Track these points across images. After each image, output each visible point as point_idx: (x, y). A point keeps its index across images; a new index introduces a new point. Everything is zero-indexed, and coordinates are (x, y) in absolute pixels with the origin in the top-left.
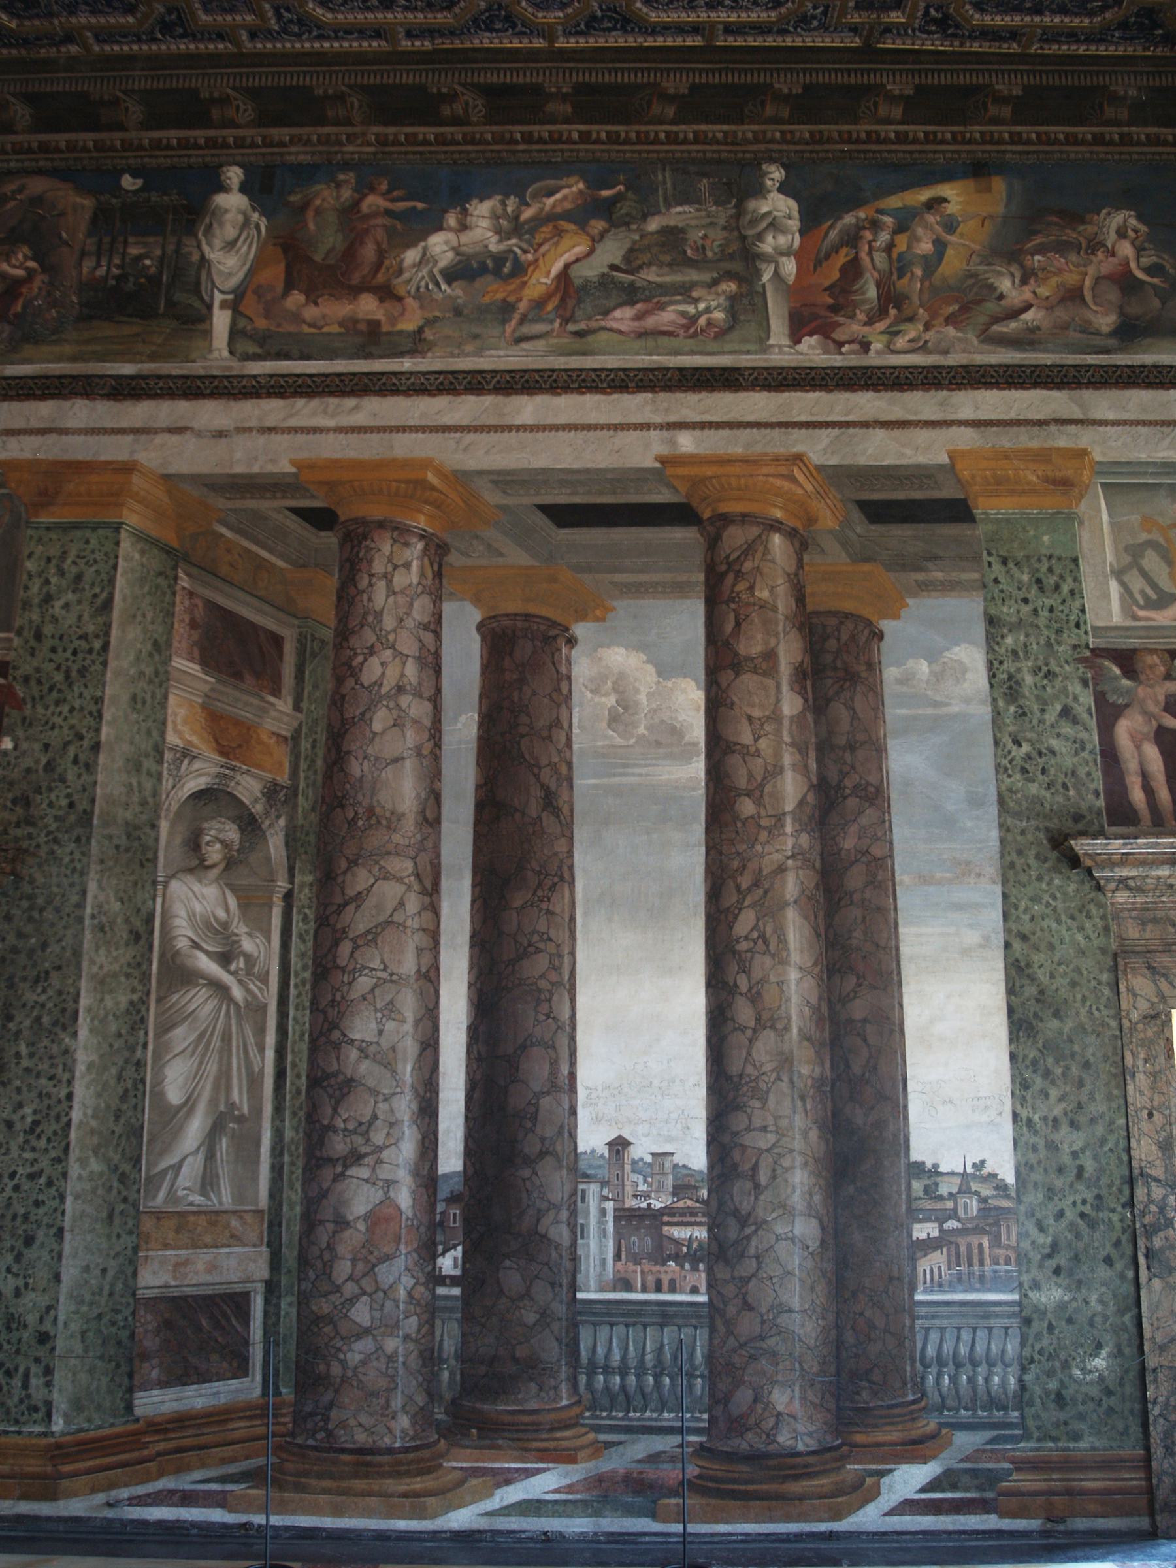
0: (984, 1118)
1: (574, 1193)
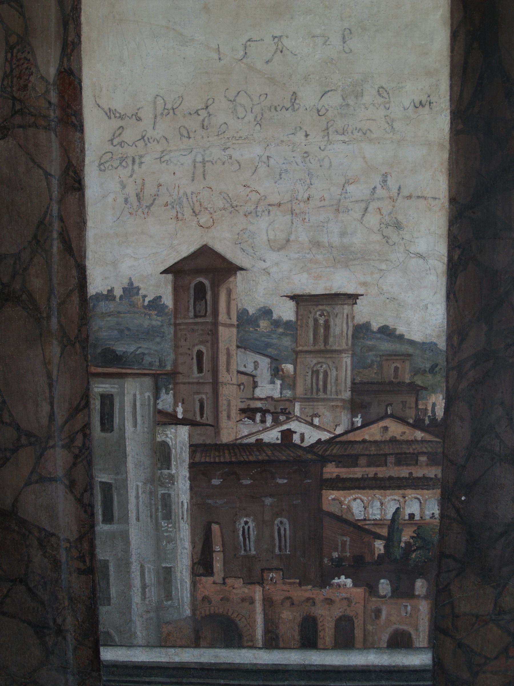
1: (82, 403)
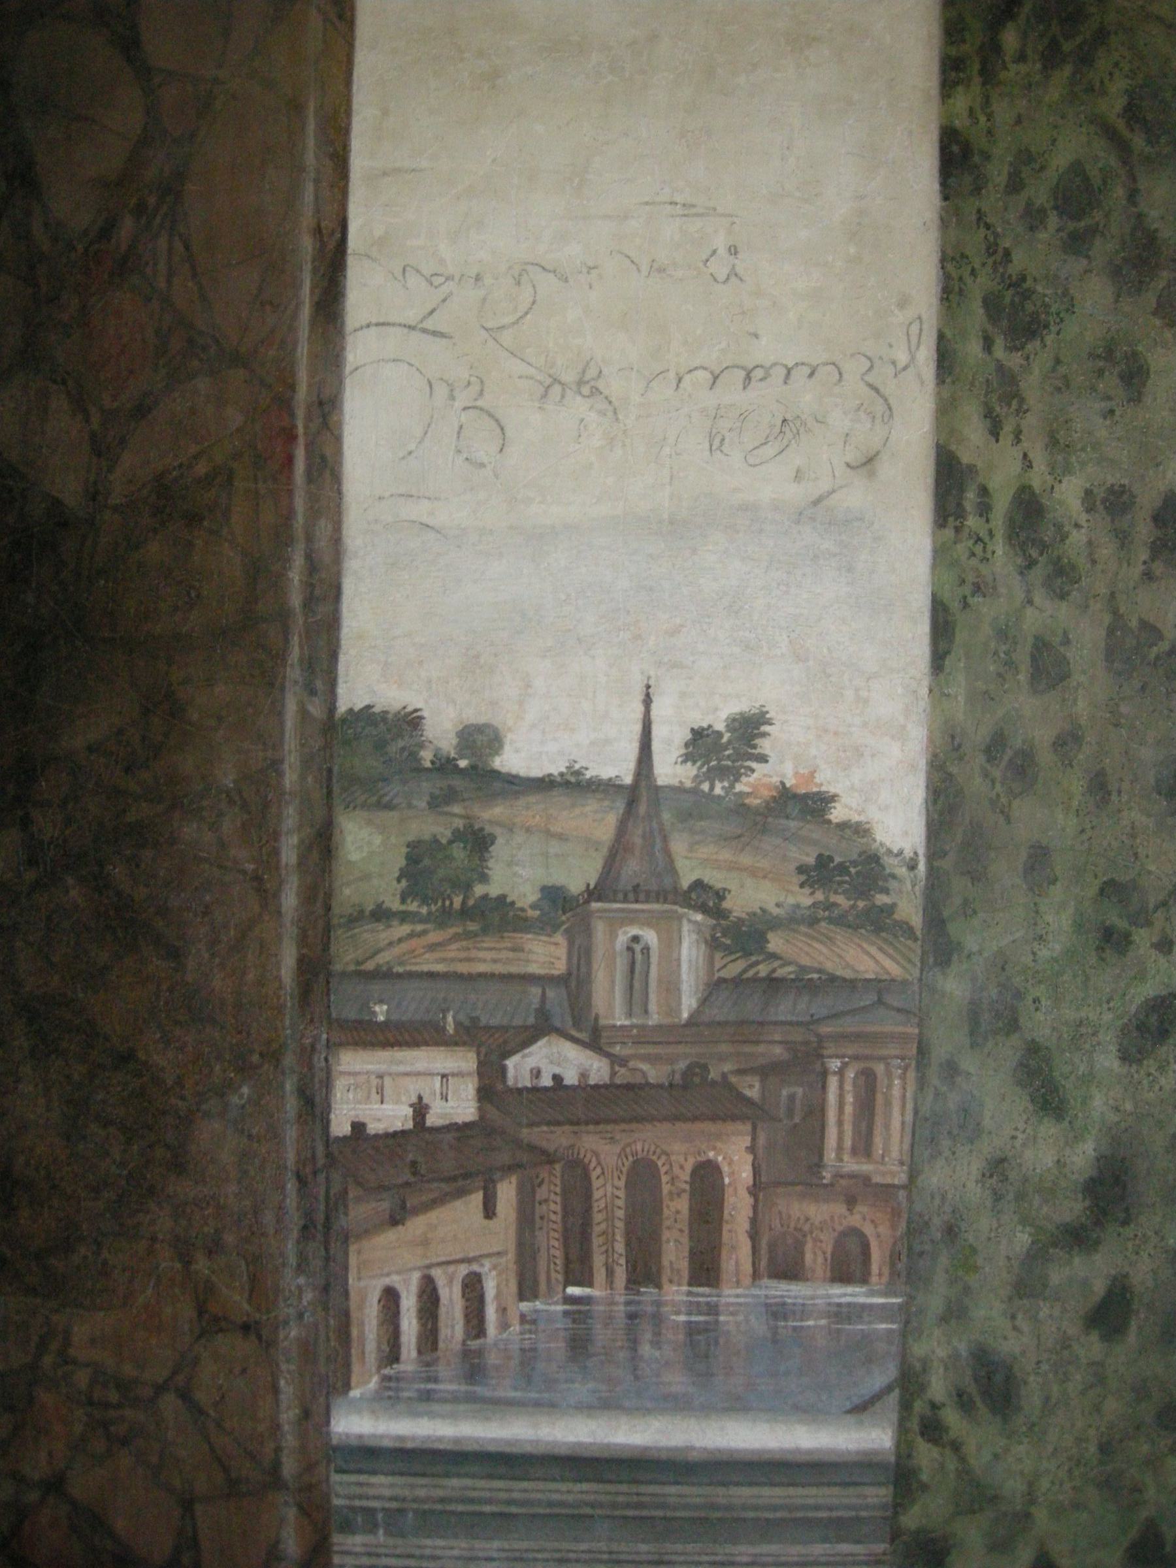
0: (774, 484)
